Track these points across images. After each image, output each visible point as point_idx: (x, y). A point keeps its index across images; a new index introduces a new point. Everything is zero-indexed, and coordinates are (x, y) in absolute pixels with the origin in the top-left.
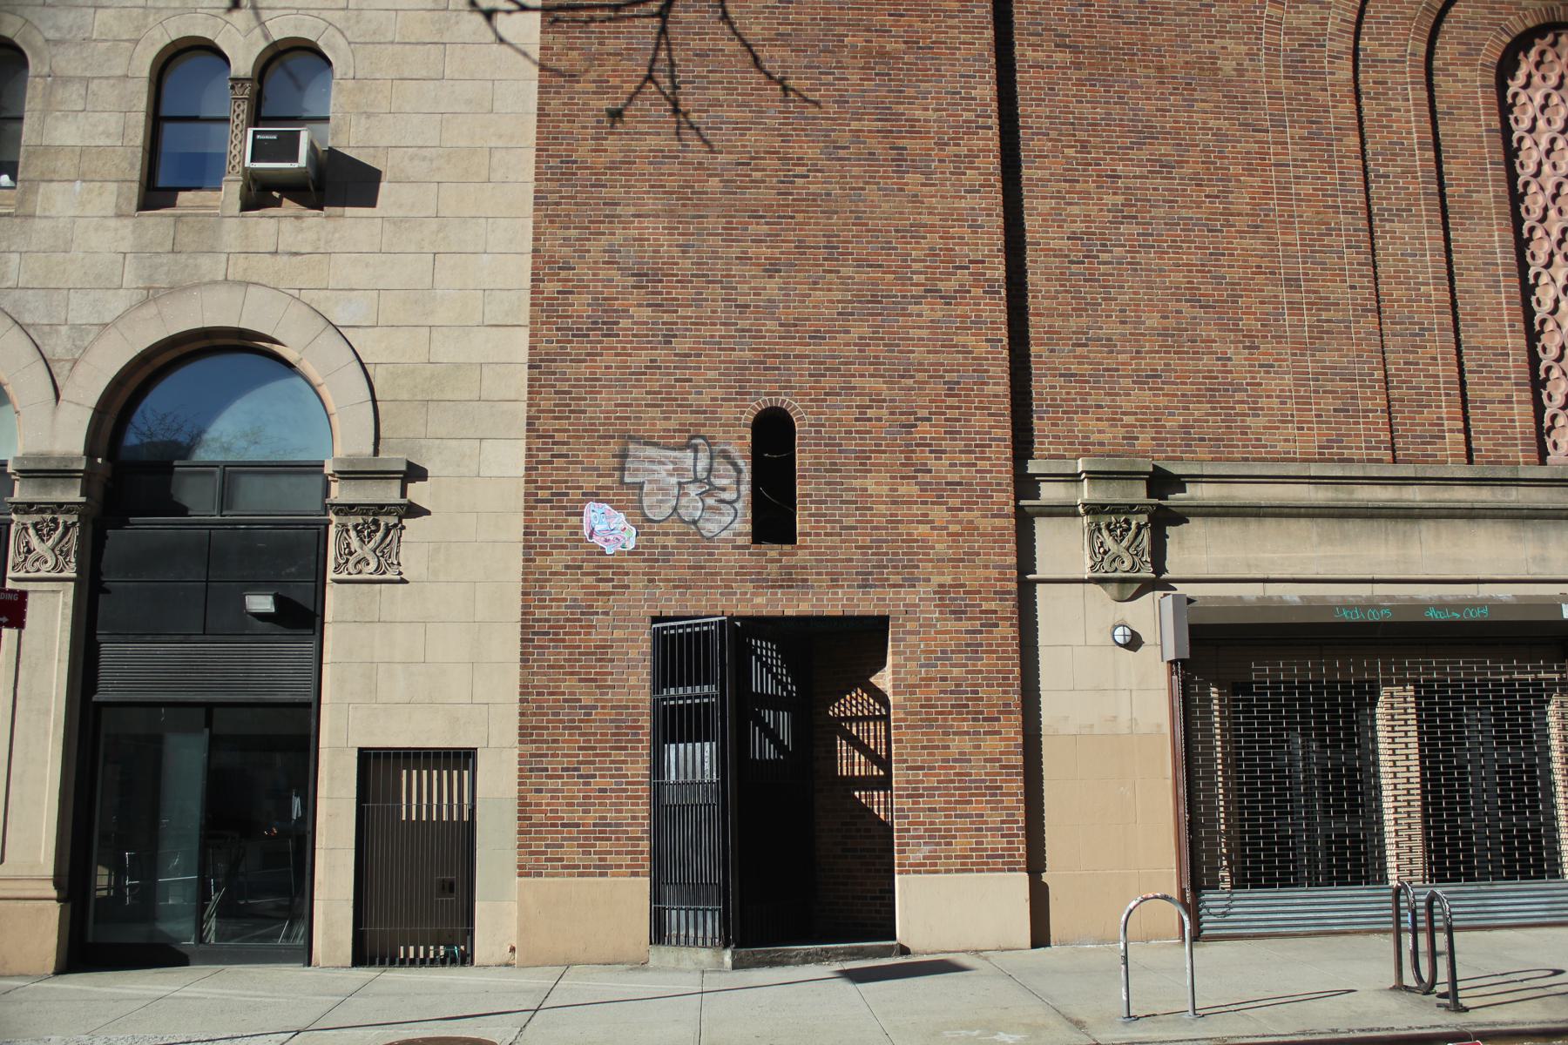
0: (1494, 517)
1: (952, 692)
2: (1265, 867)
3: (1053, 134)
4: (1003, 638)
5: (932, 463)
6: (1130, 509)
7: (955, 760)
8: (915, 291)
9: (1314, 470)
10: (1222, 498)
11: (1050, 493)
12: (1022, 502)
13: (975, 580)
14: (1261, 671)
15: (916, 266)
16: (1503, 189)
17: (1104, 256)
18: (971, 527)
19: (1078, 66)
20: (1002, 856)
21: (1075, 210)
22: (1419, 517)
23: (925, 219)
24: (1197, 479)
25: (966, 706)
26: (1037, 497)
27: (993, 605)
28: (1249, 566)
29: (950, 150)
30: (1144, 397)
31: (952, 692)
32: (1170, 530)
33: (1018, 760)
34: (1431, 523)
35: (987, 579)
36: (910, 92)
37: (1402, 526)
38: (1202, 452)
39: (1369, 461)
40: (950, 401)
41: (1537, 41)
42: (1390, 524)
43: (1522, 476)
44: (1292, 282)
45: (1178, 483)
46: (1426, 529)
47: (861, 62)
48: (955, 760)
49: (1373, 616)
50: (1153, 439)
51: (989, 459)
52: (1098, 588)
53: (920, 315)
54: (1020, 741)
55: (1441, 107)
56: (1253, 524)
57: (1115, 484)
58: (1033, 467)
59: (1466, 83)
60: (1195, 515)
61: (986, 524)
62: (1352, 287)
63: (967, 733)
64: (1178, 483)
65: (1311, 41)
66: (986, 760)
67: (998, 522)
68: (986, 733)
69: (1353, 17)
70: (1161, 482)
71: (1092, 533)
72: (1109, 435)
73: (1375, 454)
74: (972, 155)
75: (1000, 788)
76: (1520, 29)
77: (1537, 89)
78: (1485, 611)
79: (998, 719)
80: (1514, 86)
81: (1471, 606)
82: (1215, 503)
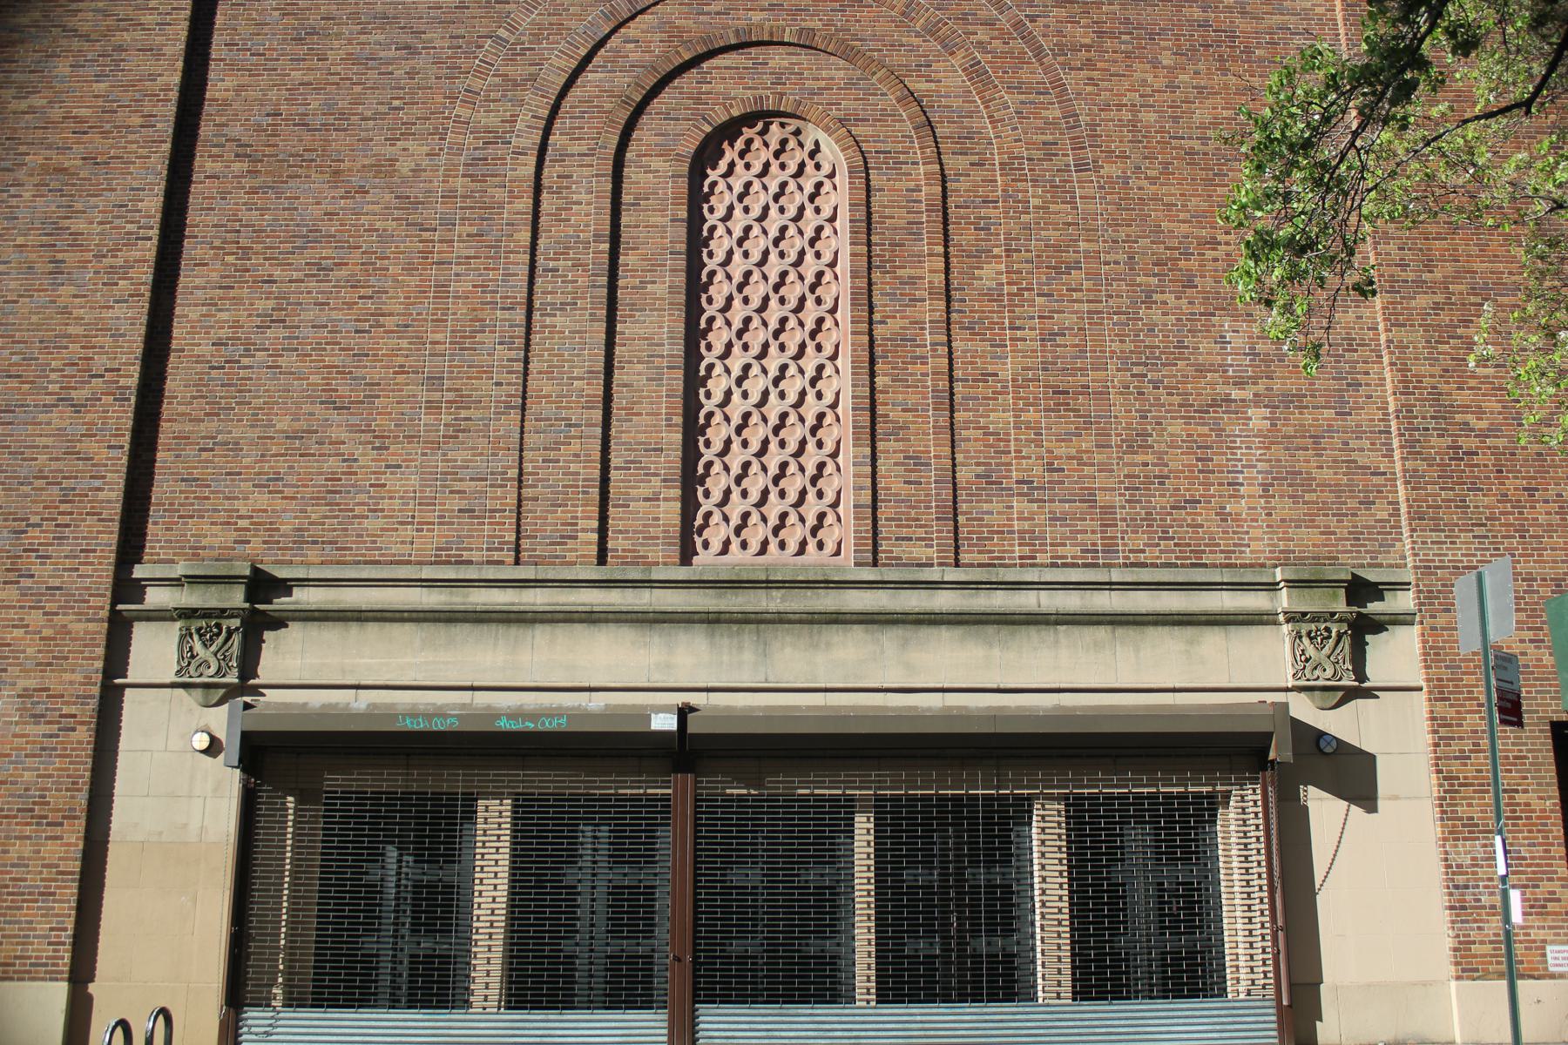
0: (617, 621)
1: (20, 796)
2: (339, 982)
3: (217, 243)
4: (79, 742)
5: (36, 569)
6: (222, 613)
7: (13, 865)
8: (49, 400)
9: (427, 572)
10: (333, 602)
11: (156, 597)
12: (120, 607)
13: (61, 683)
14: (335, 781)
15: (54, 376)
16: (681, 280)
17: (245, 361)
18: (64, 630)
19: (253, 173)
20: (46, 965)
21: (224, 316)
22: (534, 621)
23: (71, 330)
24: (304, 582)
25: (32, 810)
26: (141, 601)
27: (73, 710)
28: (343, 672)
29: (107, 261)
30: (261, 499)
31: (20, 796)
32: (267, 635)
33: (76, 866)
34: (547, 628)
35: (71, 683)
36: (79, 206)
37: (514, 631)
38: (312, 554)
39: (489, 563)
40: (64, 507)
41: (744, 130)
42: (502, 629)
43: (654, 577)
44: (435, 381)
45: (285, 586)
46: (541, 633)
47: (36, 179)
48: (13, 865)
49: (439, 725)
50: (265, 542)
51: (92, 564)
52: (181, 691)
53: (49, 424)
54: (81, 847)
55: (626, 198)
56: (354, 628)
57: (213, 588)
58: (139, 572)
59: (656, 174)
60: (294, 620)
61: (79, 627)
62: (497, 384)
63: (29, 838)
64: (285, 586)
65: (494, 138)
66: (43, 866)
67: (92, 626)
68: (47, 838)
69: (545, 113)
70: (262, 585)
71: (182, 637)
72: (217, 538)
73: (496, 556)
74: (128, 266)
75: (53, 894)
76: (724, 118)
77: (809, 177)
78: (564, 721)
79: (61, 824)
80: (713, 175)
81: (547, 716)
82: (314, 607)
